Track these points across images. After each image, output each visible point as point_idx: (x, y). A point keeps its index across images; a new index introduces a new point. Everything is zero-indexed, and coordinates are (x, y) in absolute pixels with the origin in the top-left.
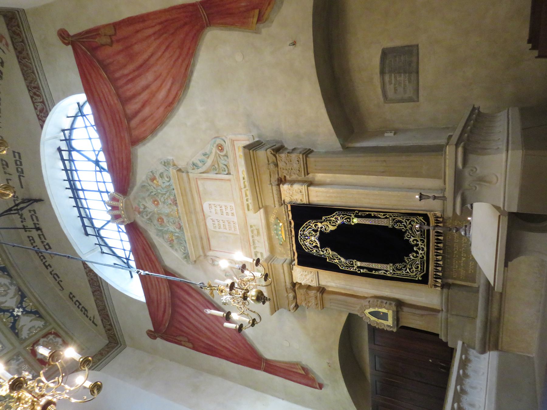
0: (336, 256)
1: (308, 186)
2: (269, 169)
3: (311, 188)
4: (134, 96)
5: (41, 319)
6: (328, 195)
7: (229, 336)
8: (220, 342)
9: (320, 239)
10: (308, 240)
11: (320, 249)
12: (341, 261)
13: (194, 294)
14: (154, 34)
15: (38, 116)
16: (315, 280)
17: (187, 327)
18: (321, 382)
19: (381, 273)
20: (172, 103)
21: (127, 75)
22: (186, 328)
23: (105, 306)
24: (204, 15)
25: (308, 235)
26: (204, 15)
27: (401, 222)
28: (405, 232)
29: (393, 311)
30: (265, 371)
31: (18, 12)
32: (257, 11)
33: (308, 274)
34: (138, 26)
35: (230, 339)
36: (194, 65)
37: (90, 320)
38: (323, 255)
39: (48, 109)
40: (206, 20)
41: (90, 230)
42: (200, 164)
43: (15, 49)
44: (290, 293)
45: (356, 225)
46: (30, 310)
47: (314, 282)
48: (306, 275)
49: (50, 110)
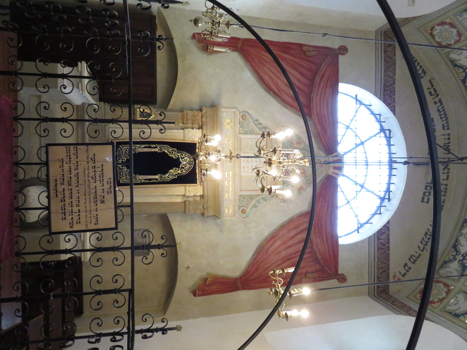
1: (185, 195)
2: (208, 205)
5: (452, 59)
7: (265, 66)
9: (180, 163)
10: (187, 161)
11: (180, 157)
12: (167, 150)
15: (389, 230)
16: (186, 134)
17: (304, 67)
18: (194, 41)
19: (143, 146)
20: (272, 238)
23: (385, 71)
24: (239, 284)
25: (187, 164)
26: (239, 284)
30: (239, 39)
31: (374, 295)
32: (207, 283)
33: (190, 137)
35: (265, 63)
36: (251, 259)
38: (178, 153)
39: (376, 235)
40: (238, 281)
41: (387, 132)
42: (261, 200)
43: (388, 274)
44: (205, 121)
46: (460, 69)
48: (192, 136)
49: (374, 234)
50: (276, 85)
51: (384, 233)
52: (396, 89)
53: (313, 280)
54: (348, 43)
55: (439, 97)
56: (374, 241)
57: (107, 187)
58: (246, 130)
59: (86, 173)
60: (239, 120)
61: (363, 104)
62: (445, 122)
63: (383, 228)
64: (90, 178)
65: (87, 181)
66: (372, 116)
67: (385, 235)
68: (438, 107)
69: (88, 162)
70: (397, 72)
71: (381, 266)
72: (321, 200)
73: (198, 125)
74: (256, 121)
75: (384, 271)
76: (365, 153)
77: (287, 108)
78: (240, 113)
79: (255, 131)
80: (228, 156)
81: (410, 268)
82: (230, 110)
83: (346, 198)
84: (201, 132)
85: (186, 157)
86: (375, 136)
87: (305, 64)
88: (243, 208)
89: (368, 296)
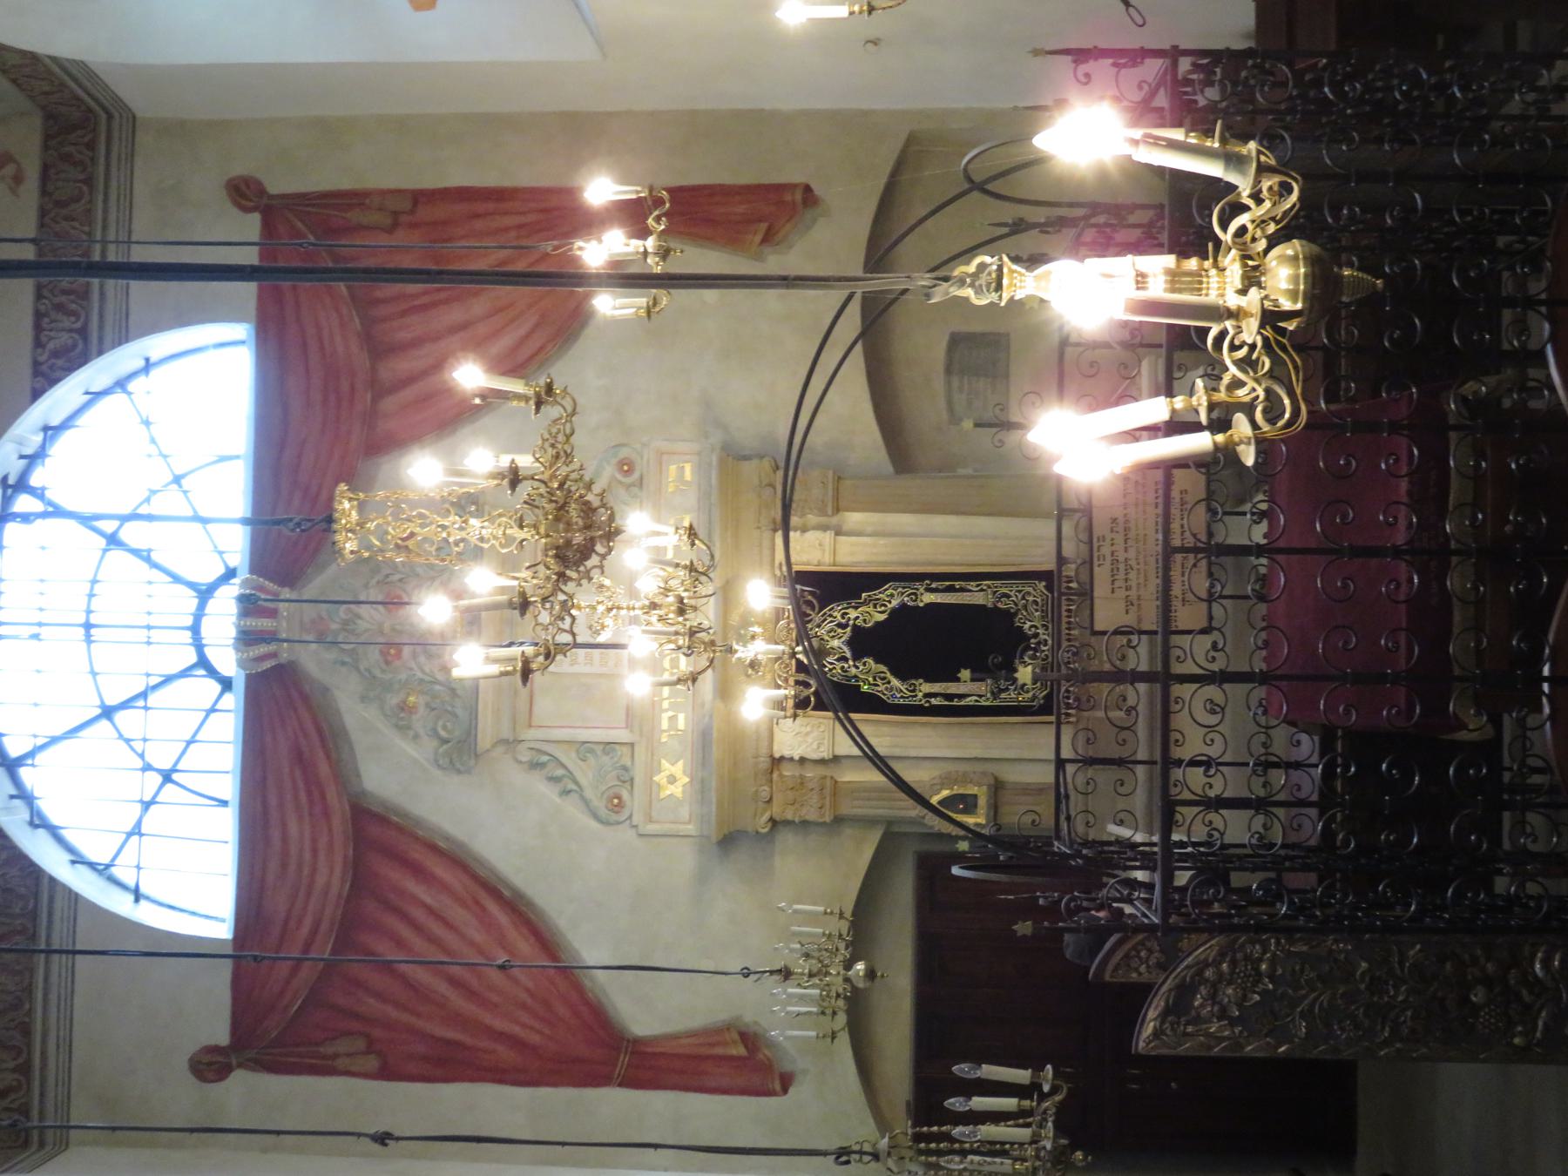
0: (882, 675)
3: (842, 539)
6: (875, 551)
7: (528, 990)
8: (488, 1018)
9: (850, 643)
11: (851, 663)
14: (520, 227)
15: (36, 364)
16: (826, 742)
17: (379, 996)
18: (787, 1067)
19: (969, 701)
22: (372, 1001)
23: (29, 990)
25: (827, 638)
27: (1008, 596)
28: (1016, 614)
29: (989, 786)
31: (110, 117)
32: (764, 226)
33: (811, 732)
34: (481, 207)
35: (529, 1001)
38: (856, 676)
39: (94, 349)
43: (44, 192)
45: (928, 605)
47: (822, 749)
48: (807, 734)
49: (100, 353)
50: (488, 923)
51: (56, 354)
53: (367, 201)
56: (101, 327)
57: (1106, 550)
58: (605, 759)
59: (1142, 575)
60: (631, 792)
61: (92, 866)
63: (58, 374)
64: (1135, 567)
65: (1141, 561)
66: (55, 819)
67: (51, 346)
69: (1139, 598)
71: (74, 228)
73: (781, 776)
74: (570, 791)
75: (60, 204)
76: (94, 674)
77: (448, 838)
78: (630, 817)
79: (573, 755)
80: (721, 651)
83: (187, 498)
84: (776, 748)
85: (831, 664)
86: (54, 740)
87: (372, 1005)
88: (628, 480)
89: (139, 114)
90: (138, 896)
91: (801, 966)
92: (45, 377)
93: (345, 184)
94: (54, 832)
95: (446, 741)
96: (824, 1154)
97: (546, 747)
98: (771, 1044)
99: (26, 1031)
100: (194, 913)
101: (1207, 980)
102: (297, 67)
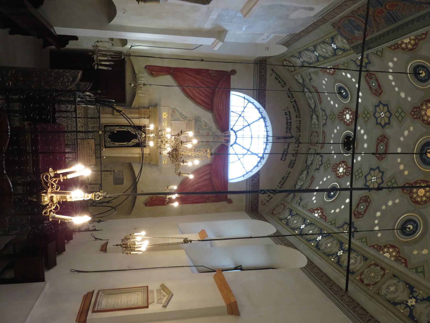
4: (206, 180)
13: (200, 101)
14: (190, 198)
18: (146, 70)
21: (205, 187)
23: (259, 84)
27: (112, 144)
28: (111, 141)
30: (171, 68)
31: (249, 211)
32: (153, 200)
37: (275, 73)
39: (251, 178)
43: (258, 200)
45: (125, 142)
49: (250, 177)
51: (256, 177)
52: (266, 95)
54: (237, 67)
55: (294, 99)
57: (93, 152)
58: (175, 118)
60: (171, 113)
61: (251, 102)
62: (298, 113)
66: (256, 109)
67: (257, 178)
68: (293, 104)
70: (267, 84)
72: (218, 158)
73: (148, 116)
75: (256, 199)
77: (199, 106)
81: (272, 198)
82: (166, 108)
86: (256, 121)
90: (244, 98)
91: (141, 86)
92: (258, 174)
93: (215, 203)
94: (256, 107)
95: (200, 121)
96: (133, 56)
97: (183, 120)
98: (148, 73)
99: (260, 78)
100: (236, 95)
101: (70, 82)
102: (221, 220)
